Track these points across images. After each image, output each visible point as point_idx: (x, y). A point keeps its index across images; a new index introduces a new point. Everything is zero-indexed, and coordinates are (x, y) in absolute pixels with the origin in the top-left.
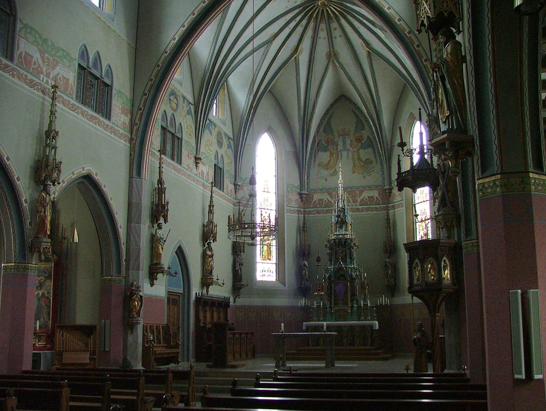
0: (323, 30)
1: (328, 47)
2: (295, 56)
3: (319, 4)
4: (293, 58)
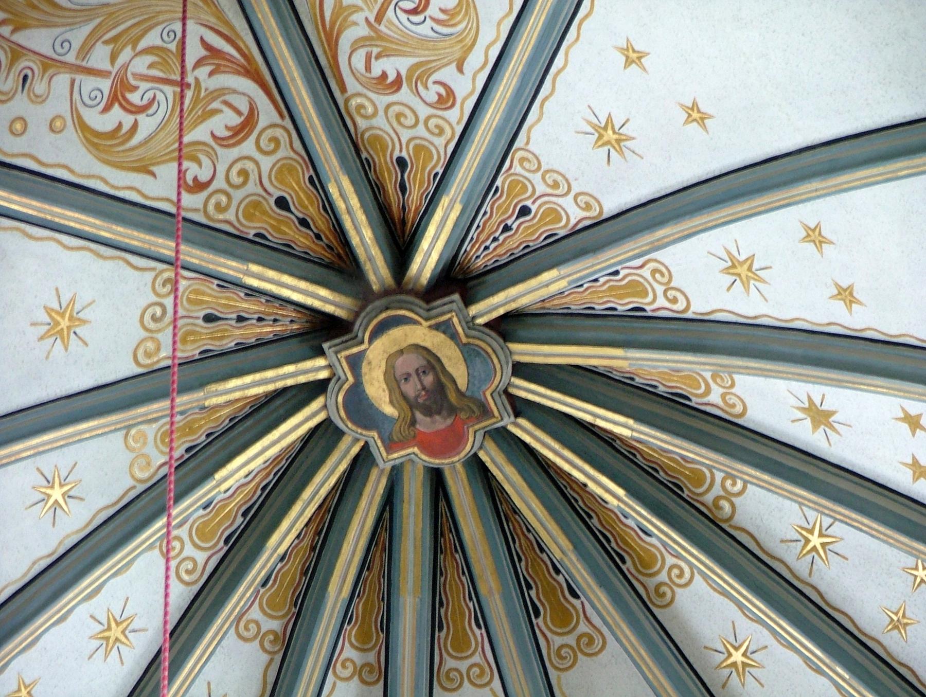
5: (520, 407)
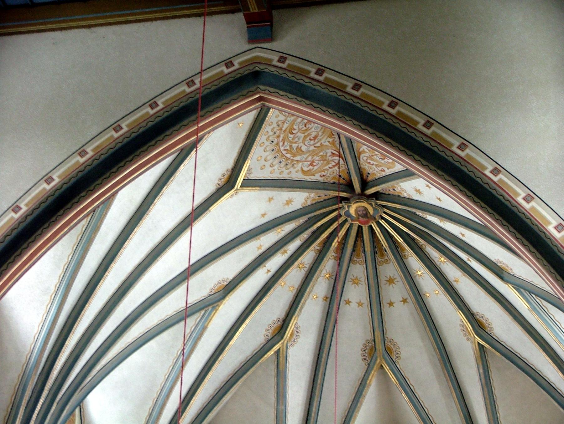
0: (356, 282)
1: (369, 327)
2: (275, 348)
3: (352, 211)
4: (271, 352)
5: (382, 218)
